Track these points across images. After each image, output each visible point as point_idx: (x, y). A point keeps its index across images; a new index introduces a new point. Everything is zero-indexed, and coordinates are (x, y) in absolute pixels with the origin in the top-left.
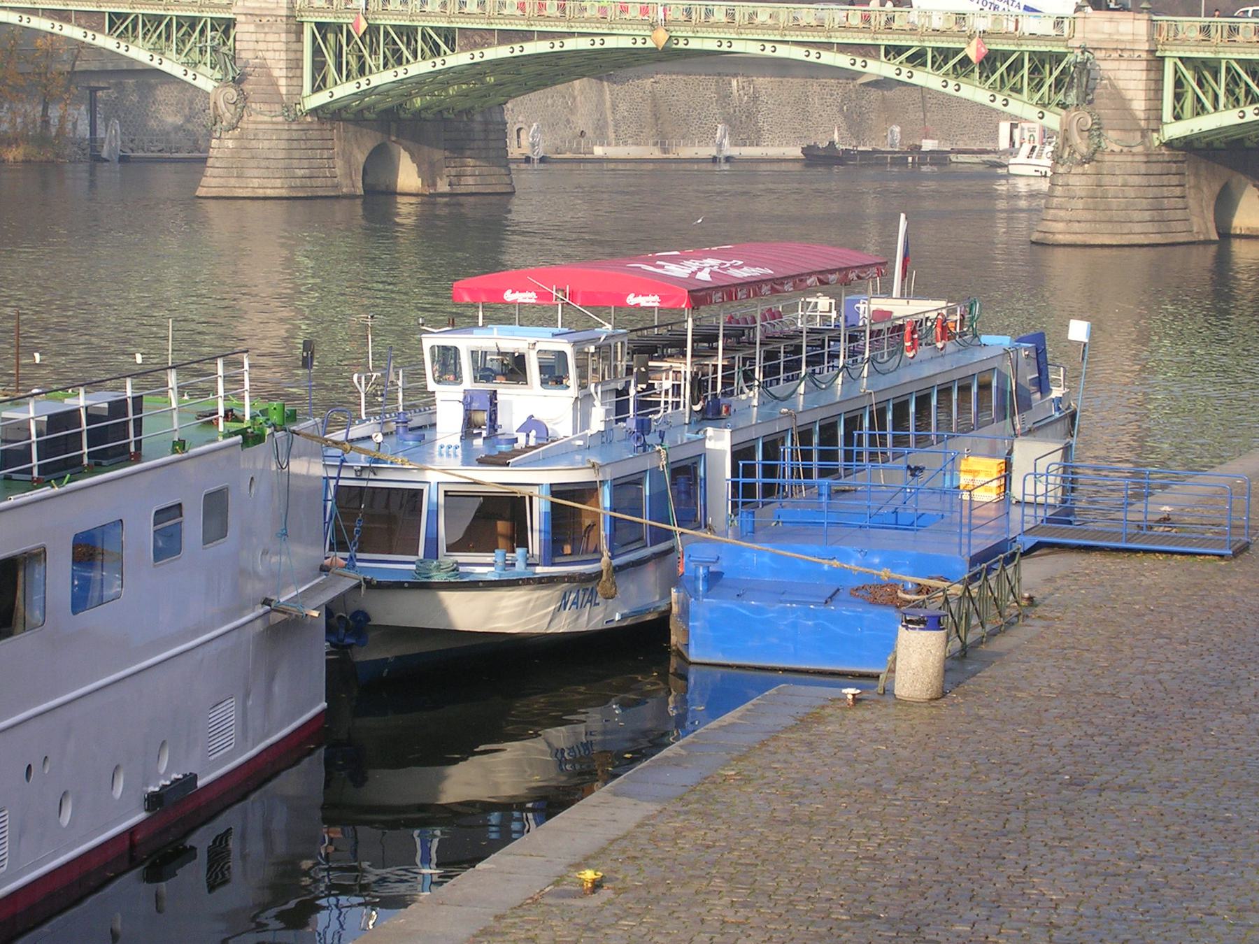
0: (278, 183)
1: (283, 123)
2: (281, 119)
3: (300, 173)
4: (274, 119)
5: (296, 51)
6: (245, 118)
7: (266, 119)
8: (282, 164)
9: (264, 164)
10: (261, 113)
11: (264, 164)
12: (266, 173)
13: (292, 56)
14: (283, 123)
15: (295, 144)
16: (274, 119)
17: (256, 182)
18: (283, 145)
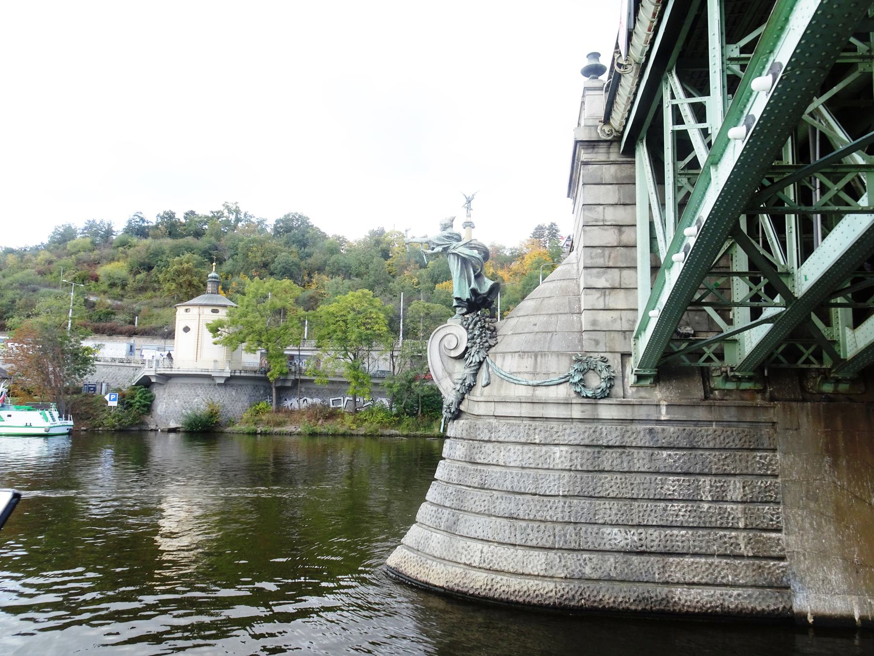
0: (537, 562)
1: (567, 403)
2: (563, 392)
3: (618, 537)
4: (541, 393)
5: (619, 227)
6: (478, 391)
7: (522, 392)
8: (557, 510)
9: (504, 506)
10: (510, 379)
11: (504, 506)
12: (501, 529)
13: (609, 237)
14: (567, 403)
15: (608, 460)
16: (541, 393)
17: (476, 552)
18: (559, 455)
